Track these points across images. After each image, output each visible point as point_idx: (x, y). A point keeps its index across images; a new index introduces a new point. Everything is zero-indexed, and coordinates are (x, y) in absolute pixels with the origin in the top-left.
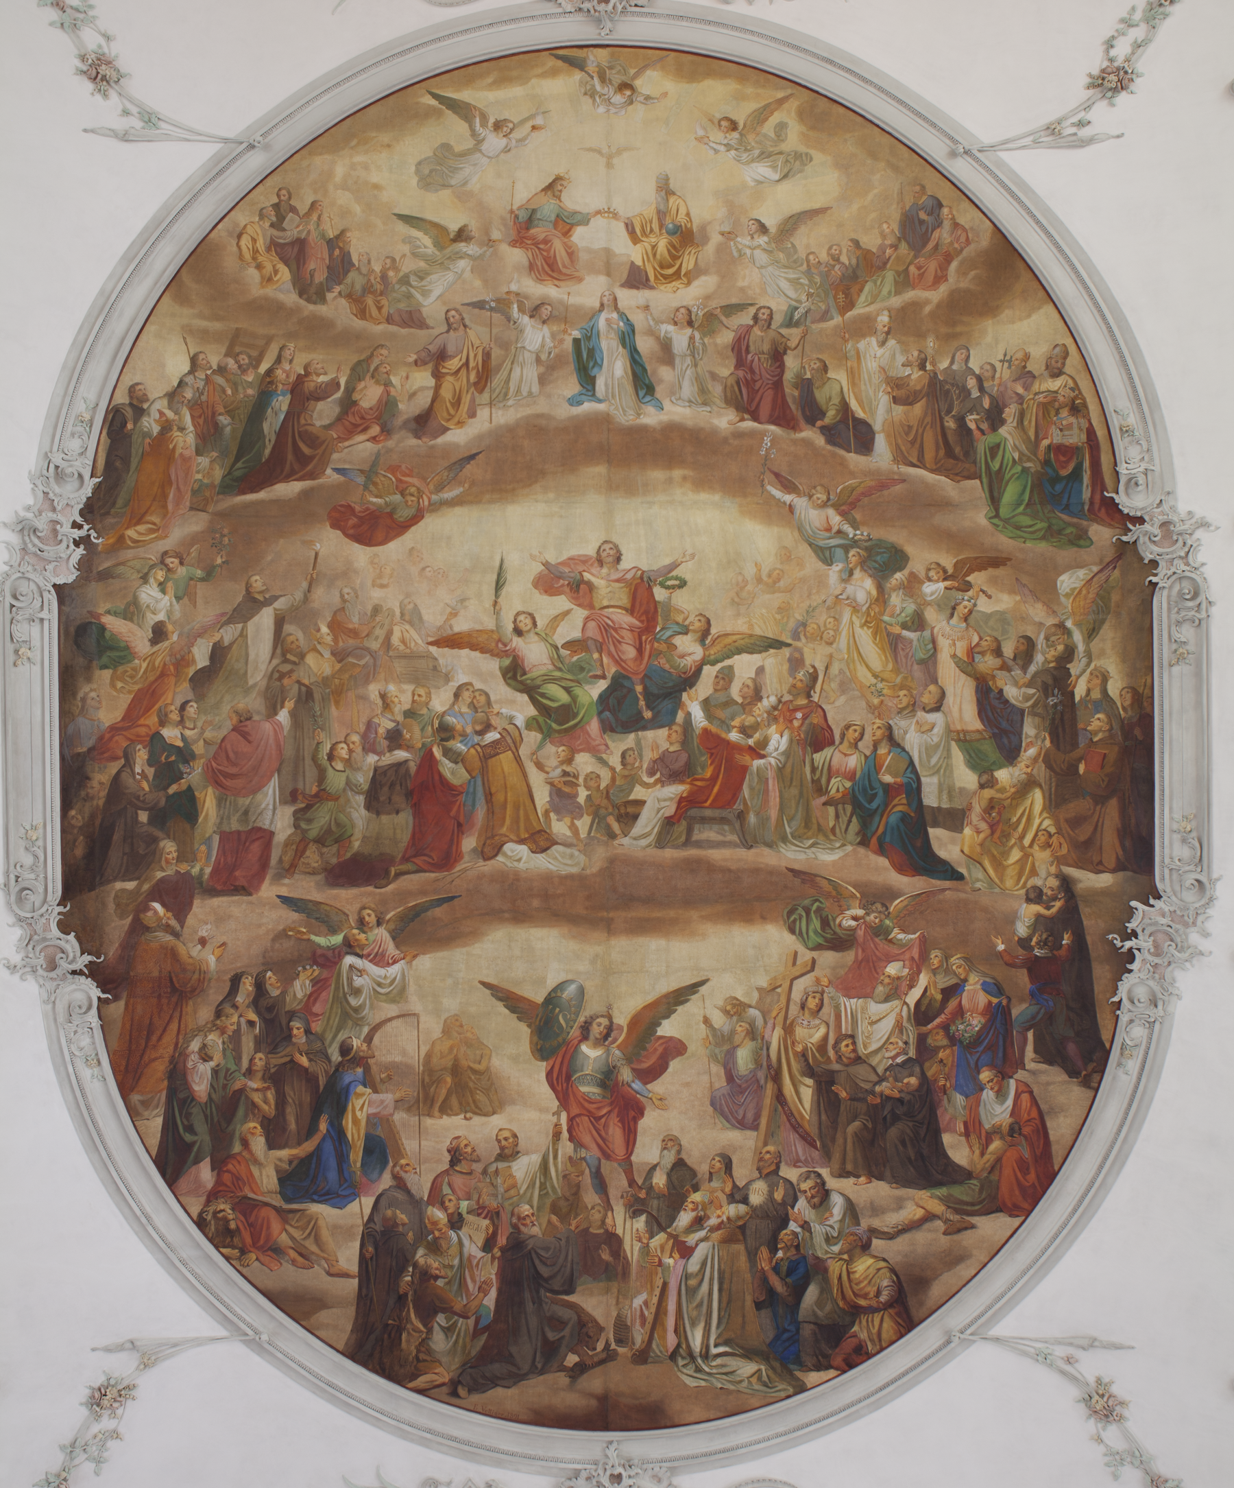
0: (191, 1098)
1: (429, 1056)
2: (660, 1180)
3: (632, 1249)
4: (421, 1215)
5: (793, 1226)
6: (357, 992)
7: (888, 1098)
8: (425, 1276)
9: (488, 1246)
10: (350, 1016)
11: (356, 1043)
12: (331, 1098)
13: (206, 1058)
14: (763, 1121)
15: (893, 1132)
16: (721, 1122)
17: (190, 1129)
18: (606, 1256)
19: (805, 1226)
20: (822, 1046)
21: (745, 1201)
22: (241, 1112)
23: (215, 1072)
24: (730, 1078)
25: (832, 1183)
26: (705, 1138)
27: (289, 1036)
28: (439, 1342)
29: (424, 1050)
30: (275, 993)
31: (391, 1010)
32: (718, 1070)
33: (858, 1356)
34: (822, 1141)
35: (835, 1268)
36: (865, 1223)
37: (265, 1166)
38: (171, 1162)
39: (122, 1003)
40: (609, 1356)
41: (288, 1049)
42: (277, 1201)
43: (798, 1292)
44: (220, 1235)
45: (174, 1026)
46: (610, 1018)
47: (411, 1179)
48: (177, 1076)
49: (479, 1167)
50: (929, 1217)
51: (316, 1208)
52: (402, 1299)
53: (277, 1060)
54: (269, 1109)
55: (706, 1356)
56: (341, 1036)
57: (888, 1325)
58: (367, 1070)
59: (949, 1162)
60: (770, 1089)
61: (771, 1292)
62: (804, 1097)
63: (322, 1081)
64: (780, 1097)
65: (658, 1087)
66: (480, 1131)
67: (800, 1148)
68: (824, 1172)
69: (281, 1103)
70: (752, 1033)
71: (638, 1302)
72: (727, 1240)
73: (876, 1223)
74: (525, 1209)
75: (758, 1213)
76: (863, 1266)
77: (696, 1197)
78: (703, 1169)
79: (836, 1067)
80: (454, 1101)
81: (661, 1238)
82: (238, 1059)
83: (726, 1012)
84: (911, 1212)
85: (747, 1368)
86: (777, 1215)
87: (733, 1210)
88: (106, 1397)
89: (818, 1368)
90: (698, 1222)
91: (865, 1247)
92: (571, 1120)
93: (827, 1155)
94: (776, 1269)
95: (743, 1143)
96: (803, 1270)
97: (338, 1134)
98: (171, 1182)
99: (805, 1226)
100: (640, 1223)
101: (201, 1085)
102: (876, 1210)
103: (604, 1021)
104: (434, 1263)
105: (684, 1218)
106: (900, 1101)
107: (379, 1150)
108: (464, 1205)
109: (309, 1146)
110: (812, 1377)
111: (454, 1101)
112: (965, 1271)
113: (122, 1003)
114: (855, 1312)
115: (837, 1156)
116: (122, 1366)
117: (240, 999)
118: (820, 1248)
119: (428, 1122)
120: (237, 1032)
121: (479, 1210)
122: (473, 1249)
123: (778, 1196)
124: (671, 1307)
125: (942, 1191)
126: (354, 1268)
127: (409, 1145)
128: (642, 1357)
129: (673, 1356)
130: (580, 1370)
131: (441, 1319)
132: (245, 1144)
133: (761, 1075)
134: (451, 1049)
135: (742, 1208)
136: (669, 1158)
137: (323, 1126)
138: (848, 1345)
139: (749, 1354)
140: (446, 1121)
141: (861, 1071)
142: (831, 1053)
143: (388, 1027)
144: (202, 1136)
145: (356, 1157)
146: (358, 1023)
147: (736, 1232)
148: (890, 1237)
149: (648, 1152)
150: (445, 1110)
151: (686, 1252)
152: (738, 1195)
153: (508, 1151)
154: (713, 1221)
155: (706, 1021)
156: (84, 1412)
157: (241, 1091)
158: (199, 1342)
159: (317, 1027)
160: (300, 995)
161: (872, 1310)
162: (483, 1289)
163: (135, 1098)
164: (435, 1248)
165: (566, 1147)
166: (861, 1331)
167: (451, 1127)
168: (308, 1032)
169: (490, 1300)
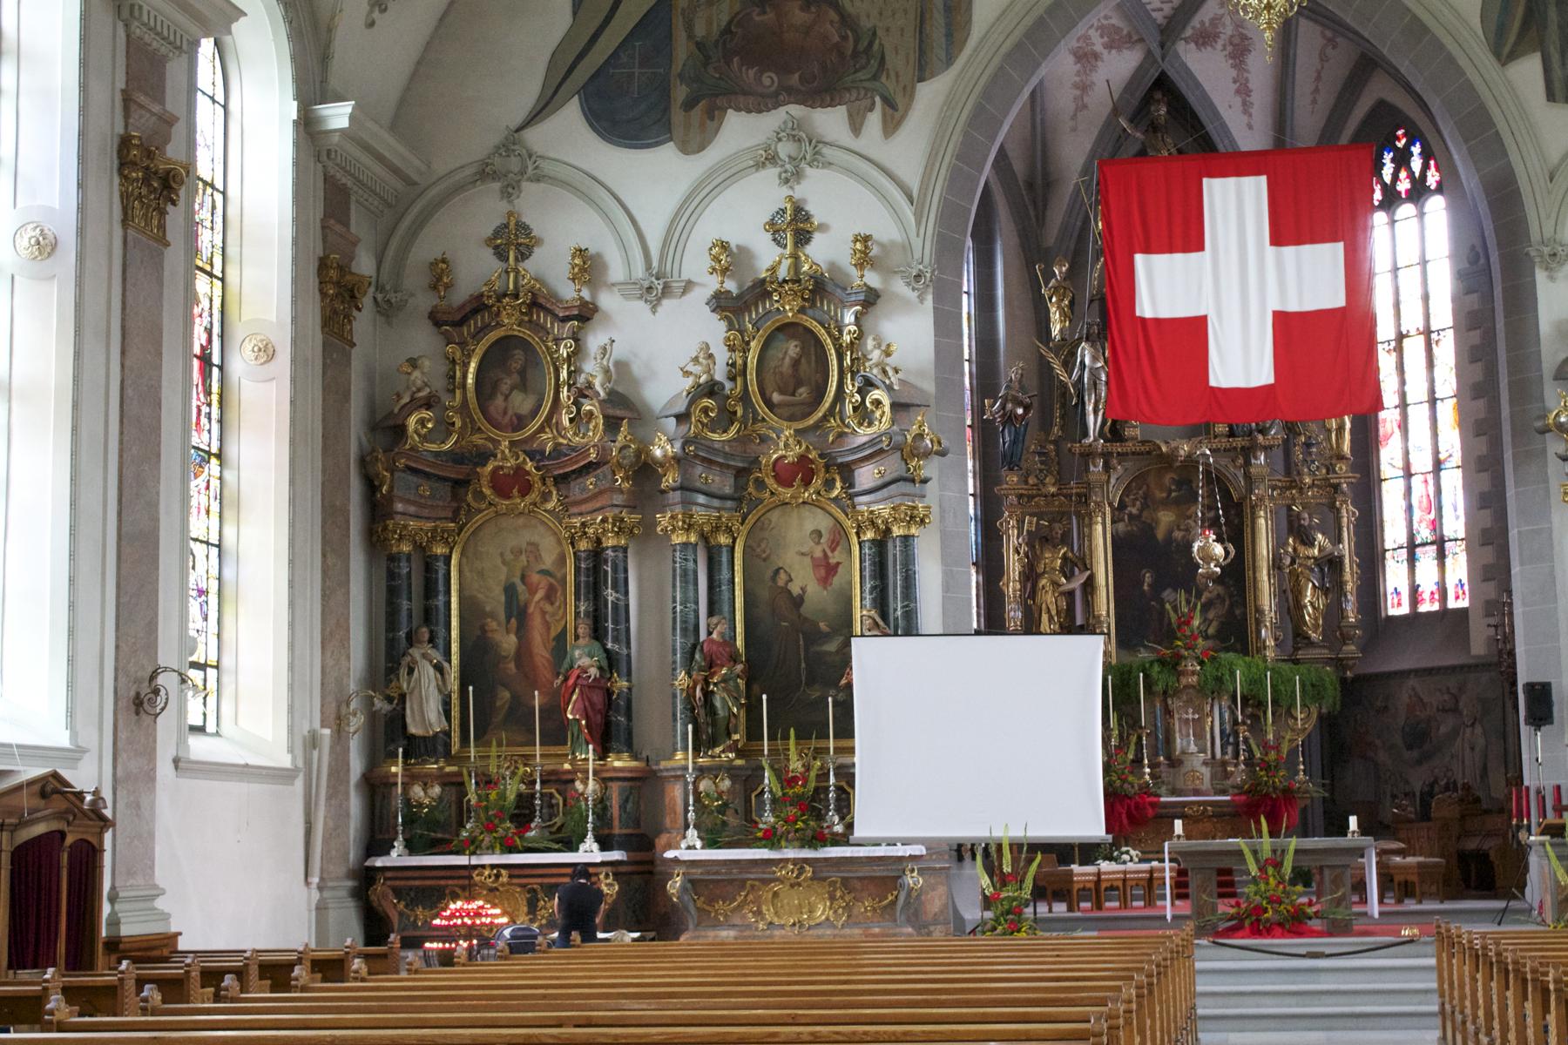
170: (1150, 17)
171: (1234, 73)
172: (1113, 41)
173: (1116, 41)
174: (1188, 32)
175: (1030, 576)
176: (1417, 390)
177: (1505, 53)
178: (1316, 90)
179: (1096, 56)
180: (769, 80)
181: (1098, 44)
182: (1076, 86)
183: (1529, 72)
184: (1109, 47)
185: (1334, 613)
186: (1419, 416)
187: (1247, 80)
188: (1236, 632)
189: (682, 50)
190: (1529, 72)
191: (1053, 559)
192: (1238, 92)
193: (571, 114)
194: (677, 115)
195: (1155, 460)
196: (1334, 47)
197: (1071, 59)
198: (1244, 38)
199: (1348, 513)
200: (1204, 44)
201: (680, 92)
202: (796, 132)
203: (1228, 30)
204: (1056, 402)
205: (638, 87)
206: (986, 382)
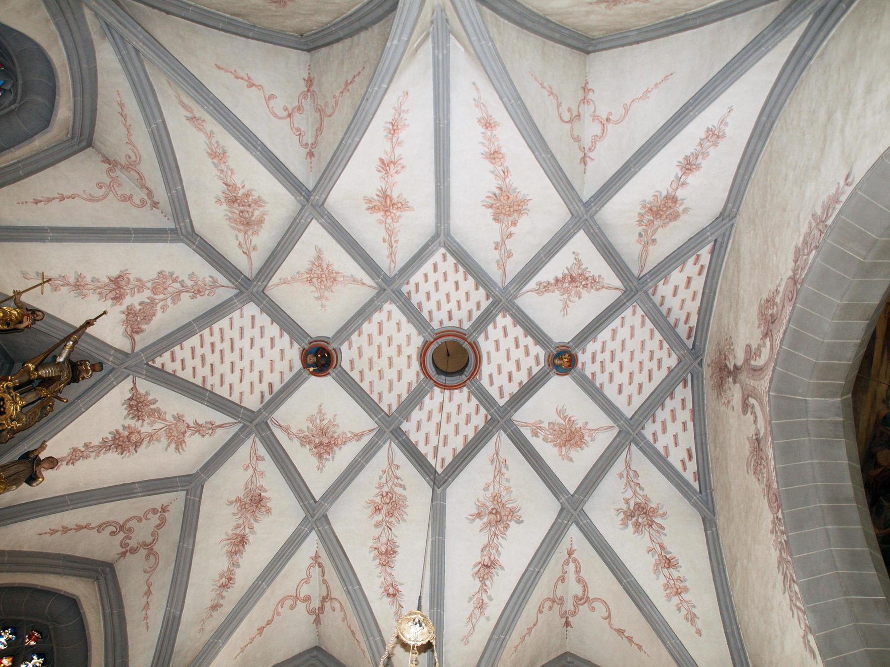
170: (165, 349)
171: (96, 441)
172: (135, 315)
173: (135, 321)
174: (144, 386)
178: (65, 530)
179: (118, 299)
181: (133, 300)
182: (79, 277)
184: (129, 312)
187: (88, 457)
192: (75, 450)
196: (113, 533)
197: (114, 273)
198: (137, 445)
200: (131, 406)
203: (146, 428)
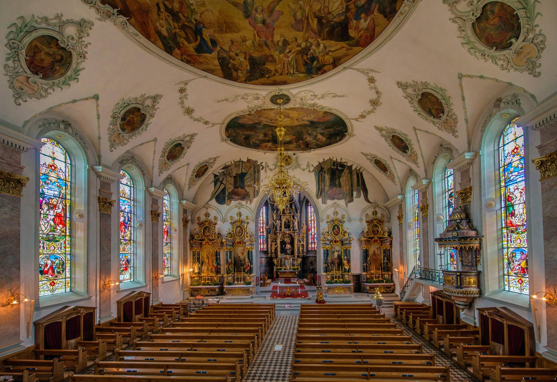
0: (164, 37)
1: (218, 19)
2: (280, 44)
3: (276, 58)
4: (229, 55)
5: (311, 51)
6: (192, 5)
7: (336, 22)
8: (234, 65)
9: (245, 58)
10: (193, 11)
11: (198, 18)
12: (198, 32)
13: (163, 27)
14: (304, 29)
15: (337, 30)
16: (294, 30)
17: (168, 43)
18: (271, 59)
19: (314, 51)
20: (320, 11)
21: (300, 47)
22: (178, 38)
23: (167, 30)
24: (296, 20)
25: (320, 42)
26: (290, 35)
27: (180, 18)
28: (240, 75)
29: (216, 18)
30: (170, 7)
31: (204, 9)
32: (292, 18)
33: (325, 72)
34: (319, 34)
35: (320, 58)
36: (328, 50)
37: (191, 47)
38: (169, 50)
39: (133, 18)
40: (275, 75)
41: (181, 21)
42: (196, 54)
43: (313, 62)
44: (188, 62)
45: (149, 20)
46: (262, 6)
47: (224, 47)
48: (159, 33)
49: (238, 44)
50: (343, 47)
51: (205, 54)
52: (230, 69)
53: (180, 24)
54: (184, 35)
55: (294, 74)
56: (193, 17)
57: (331, 67)
58: (204, 24)
59: (350, 36)
60: (306, 22)
61: (307, 63)
62: (314, 23)
63: (194, 28)
64: (308, 23)
65: (276, 24)
66: (236, 36)
67: (313, 35)
68: (319, 40)
69: (186, 34)
70: (301, 8)
71: (279, 66)
72: (297, 54)
73: (330, 49)
74: (251, 51)
75: (303, 49)
76: (327, 57)
77: (289, 47)
78: (290, 41)
79: (323, 15)
80: (228, 30)
81: (282, 55)
82: (170, 25)
83: (294, 3)
84: (338, 46)
85: (302, 75)
86: (307, 49)
87: (299, 48)
88: (182, 91)
89: (316, 74)
90: (290, 51)
91: (327, 54)
92: (257, 32)
93: (320, 36)
94: (308, 59)
95: (300, 35)
96: (314, 59)
97: (203, 39)
98: (171, 54)
99: (314, 51)
100: (277, 52)
101: (165, 33)
102: (331, 47)
103: (261, 8)
104: (235, 62)
105: (287, 51)
106: (339, 22)
107: (214, 43)
108: (238, 51)
109: (198, 42)
110: (314, 76)
111: (228, 30)
112: (349, 57)
113: (133, 18)
114: (324, 65)
115: (322, 36)
116: (182, 86)
117: (162, 10)
118: (317, 54)
119: (223, 35)
120: (166, 18)
121: (241, 52)
122: (242, 59)
123: (308, 45)
124: (286, 66)
125: (347, 42)
126: (218, 64)
127: (221, 40)
128: (281, 74)
129: (287, 74)
130: (269, 77)
131: (239, 71)
132: (183, 44)
133: (303, 18)
134: (223, 18)
135: (300, 48)
136: (282, 39)
137: (199, 38)
138: (322, 71)
139: (302, 73)
140: (227, 35)
141: (330, 16)
142: (322, 12)
143: (204, 14)
144: (172, 43)
145: (209, 44)
146: (196, 13)
147: (299, 52)
148: (333, 52)
149: (277, 38)
150: (226, 32)
151: (288, 57)
152: (299, 45)
153: (244, 40)
154: (293, 51)
155: (288, 5)
156: (180, 94)
157: (176, 32)
158: (194, 79)
159: (186, 15)
160: (177, 7)
161: (328, 65)
162: (246, 66)
163: (152, 40)
164: (234, 60)
165: (257, 38)
166: (325, 68)
167: (229, 36)
168: (184, 16)
169: (248, 68)
175: (271, 245)
176: (313, 226)
177: (318, 198)
180: (237, 197)
183: (320, 200)
185: (303, 250)
186: (313, 229)
188: (292, 253)
189: (227, 193)
190: (320, 200)
191: (274, 243)
193: (214, 200)
194: (226, 201)
195: (285, 234)
199: (305, 239)
201: (227, 198)
202: (239, 203)
204: (275, 227)
205: (221, 198)
206: (267, 224)
